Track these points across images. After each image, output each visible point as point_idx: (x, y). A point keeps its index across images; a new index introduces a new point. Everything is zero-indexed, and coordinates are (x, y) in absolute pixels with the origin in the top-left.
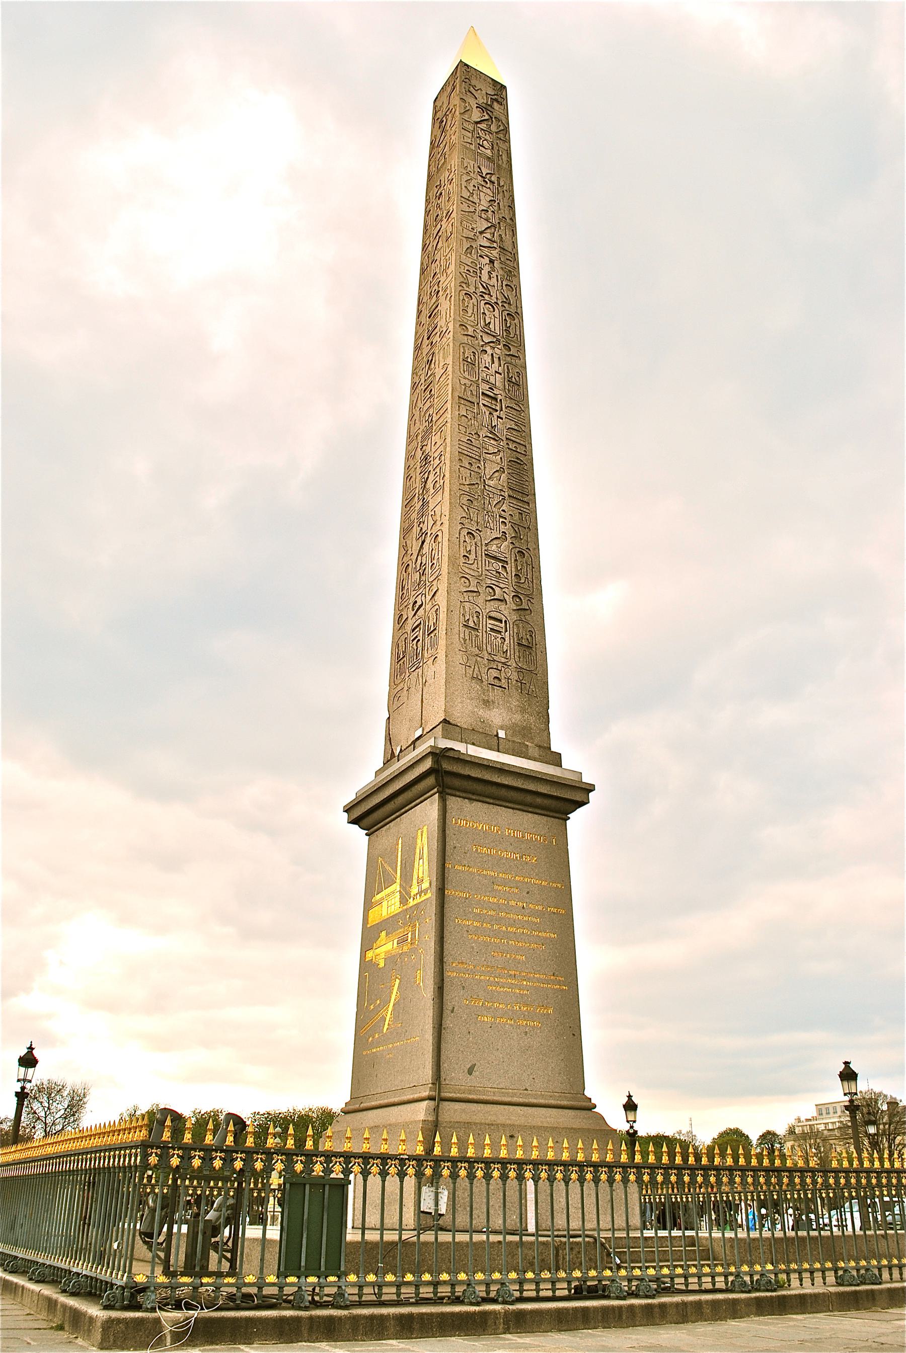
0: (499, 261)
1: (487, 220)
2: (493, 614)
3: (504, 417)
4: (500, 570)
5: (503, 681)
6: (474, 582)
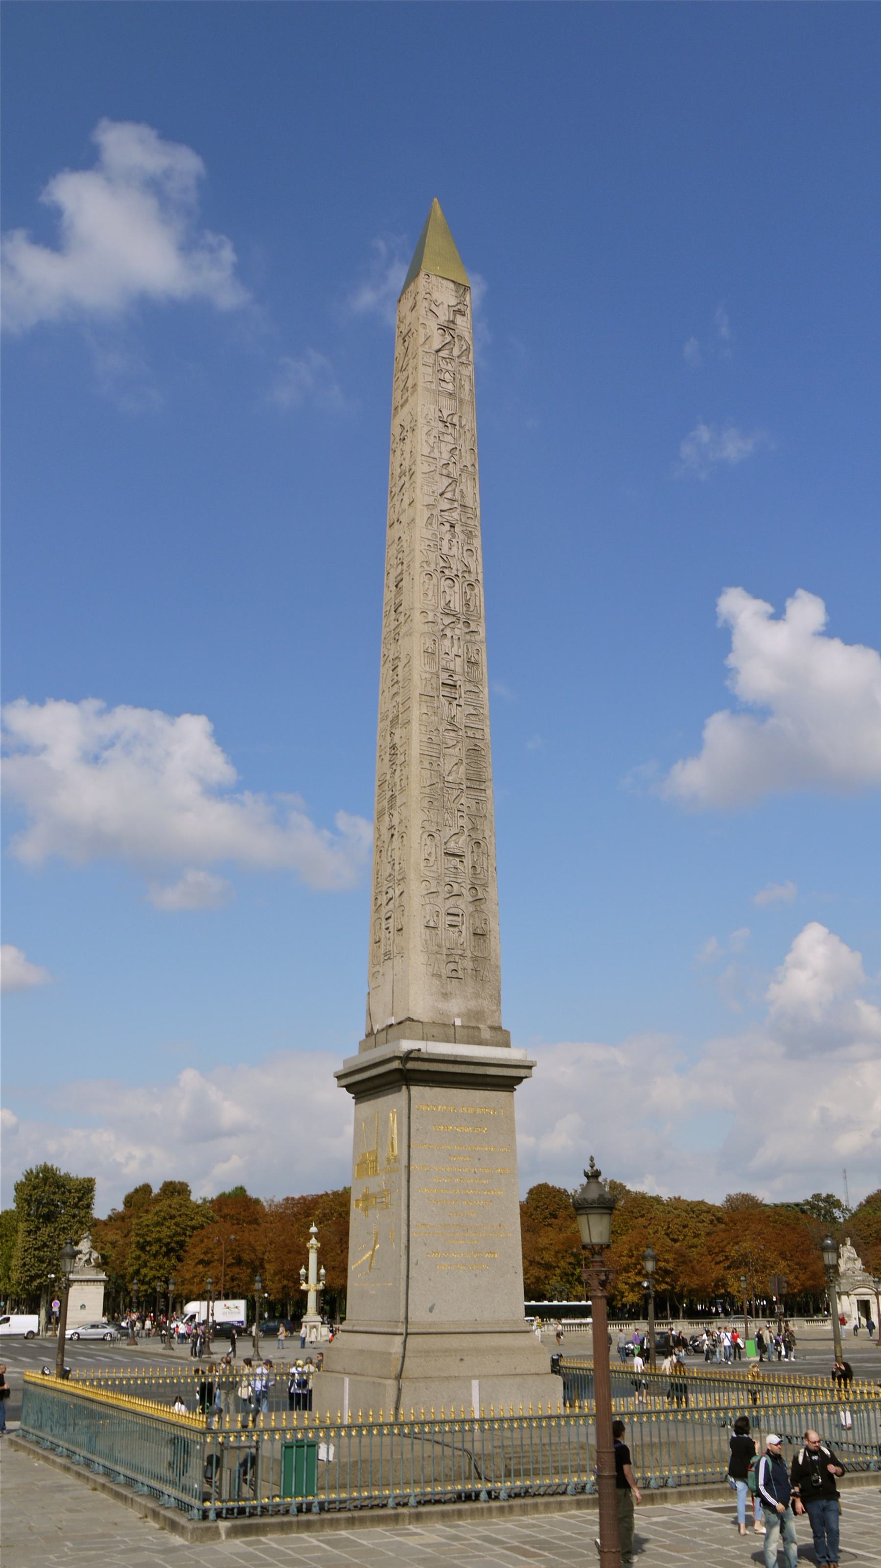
0: (460, 523)
2: (451, 911)
3: (463, 704)
5: (460, 972)
6: (434, 883)
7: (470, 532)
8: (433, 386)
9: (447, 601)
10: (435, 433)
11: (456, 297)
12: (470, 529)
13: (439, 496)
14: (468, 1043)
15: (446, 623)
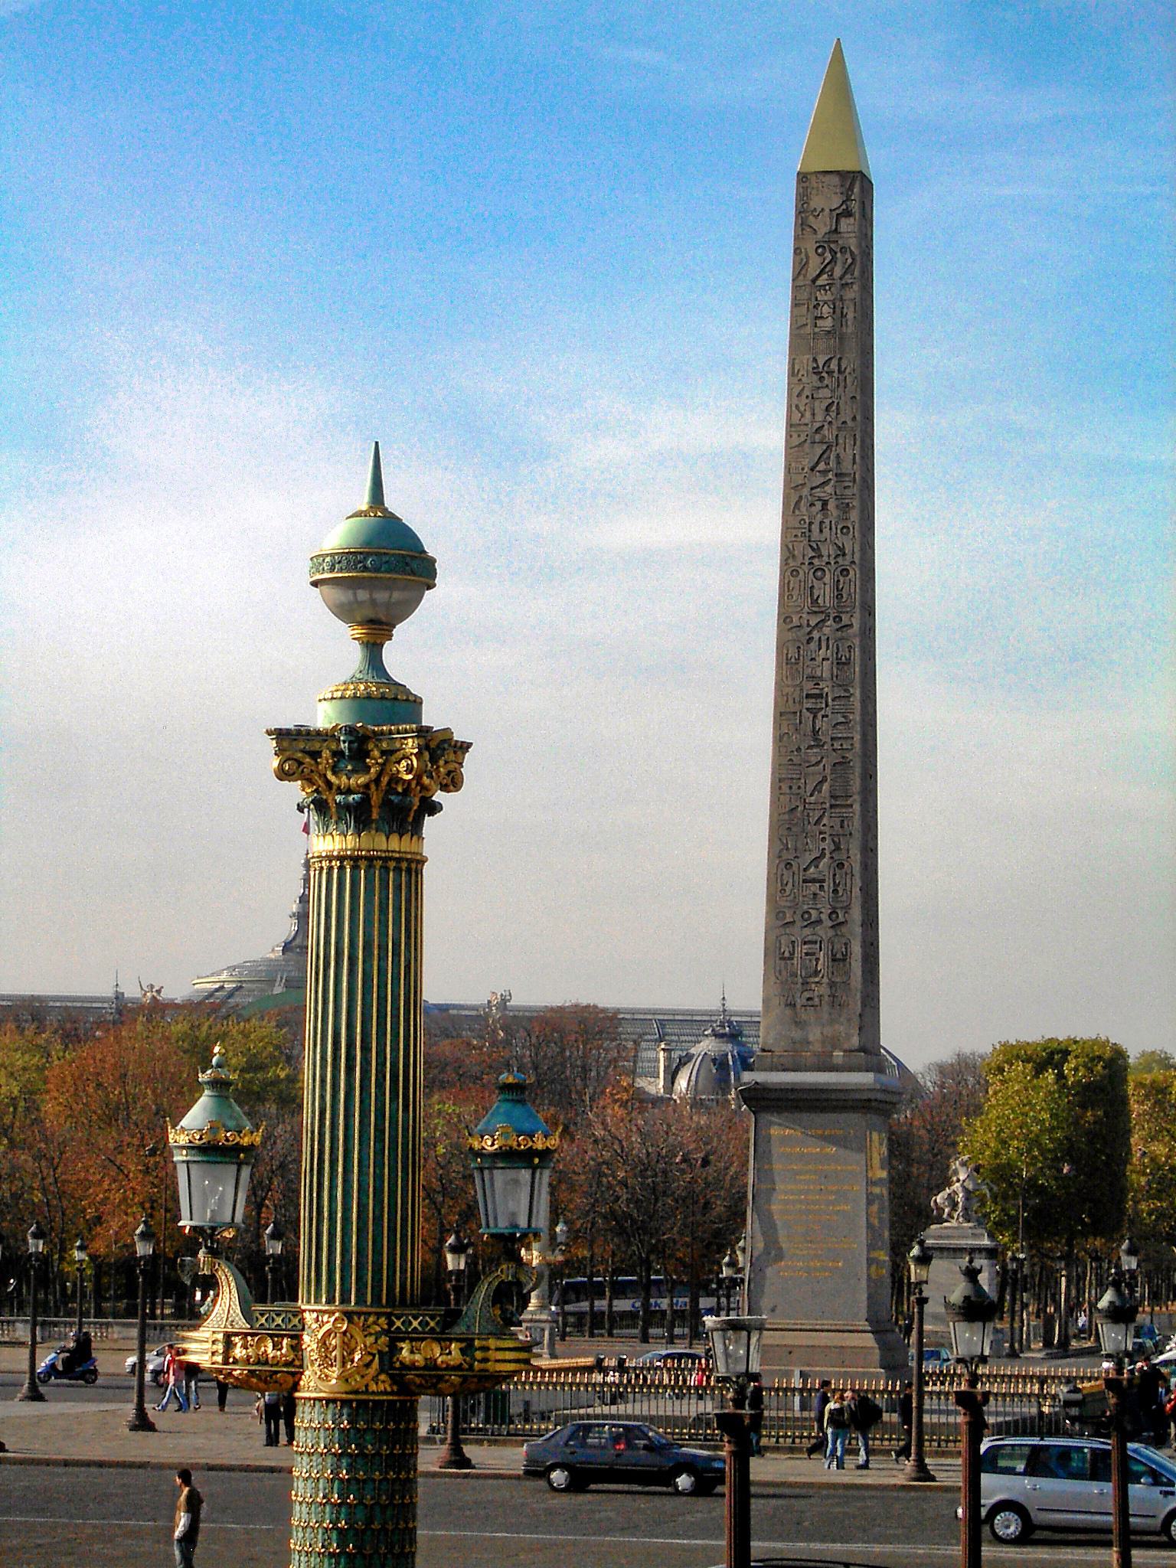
1: (821, 442)
2: (810, 938)
4: (818, 892)
7: (848, 504)
8: (808, 329)
9: (815, 597)
10: (807, 392)
11: (842, 193)
12: (847, 501)
13: (809, 471)
14: (819, 1070)
15: (813, 623)
